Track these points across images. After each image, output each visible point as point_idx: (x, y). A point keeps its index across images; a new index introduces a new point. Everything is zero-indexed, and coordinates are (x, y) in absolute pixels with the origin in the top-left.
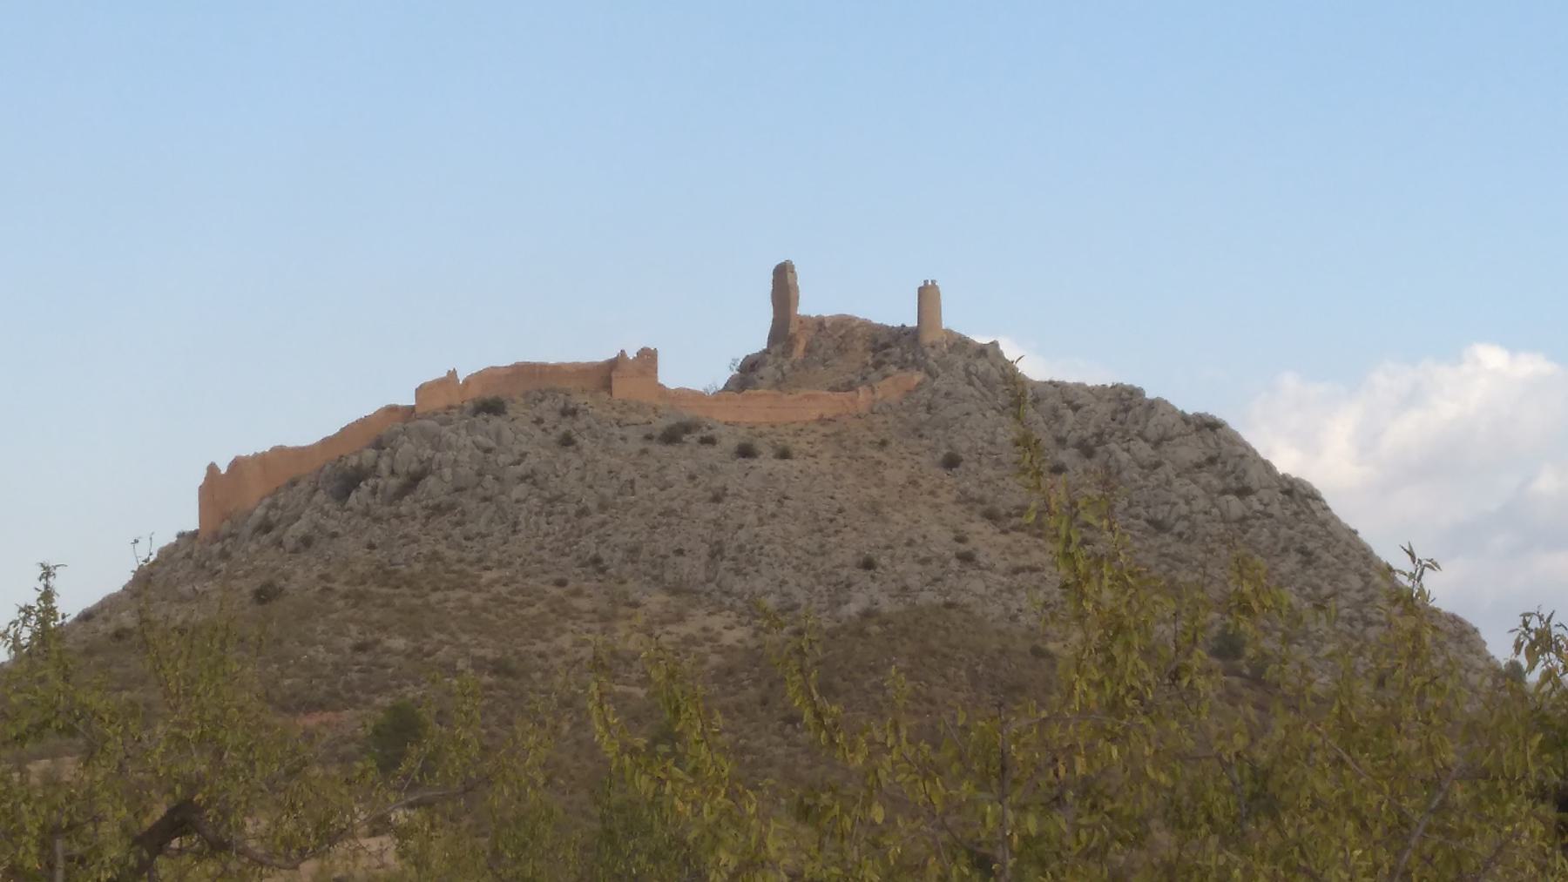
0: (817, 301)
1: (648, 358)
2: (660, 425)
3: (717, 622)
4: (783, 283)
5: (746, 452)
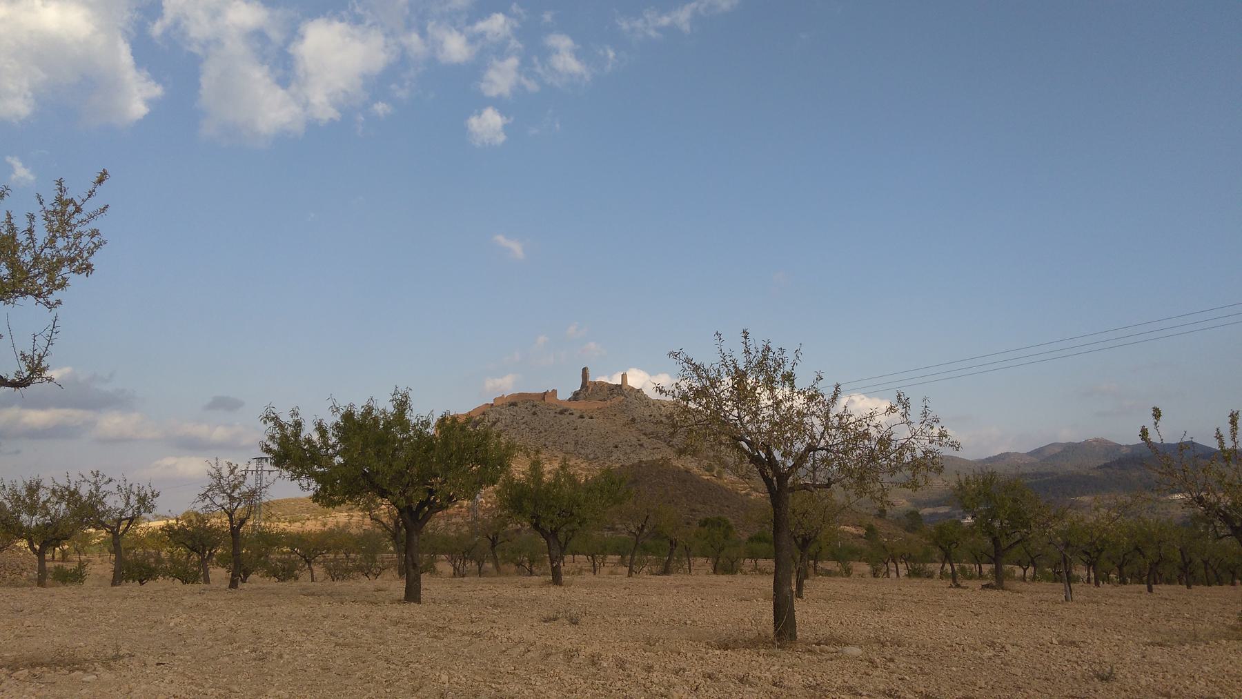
0: (596, 377)
1: (554, 392)
2: (558, 410)
3: (579, 461)
4: (585, 370)
5: (582, 417)
